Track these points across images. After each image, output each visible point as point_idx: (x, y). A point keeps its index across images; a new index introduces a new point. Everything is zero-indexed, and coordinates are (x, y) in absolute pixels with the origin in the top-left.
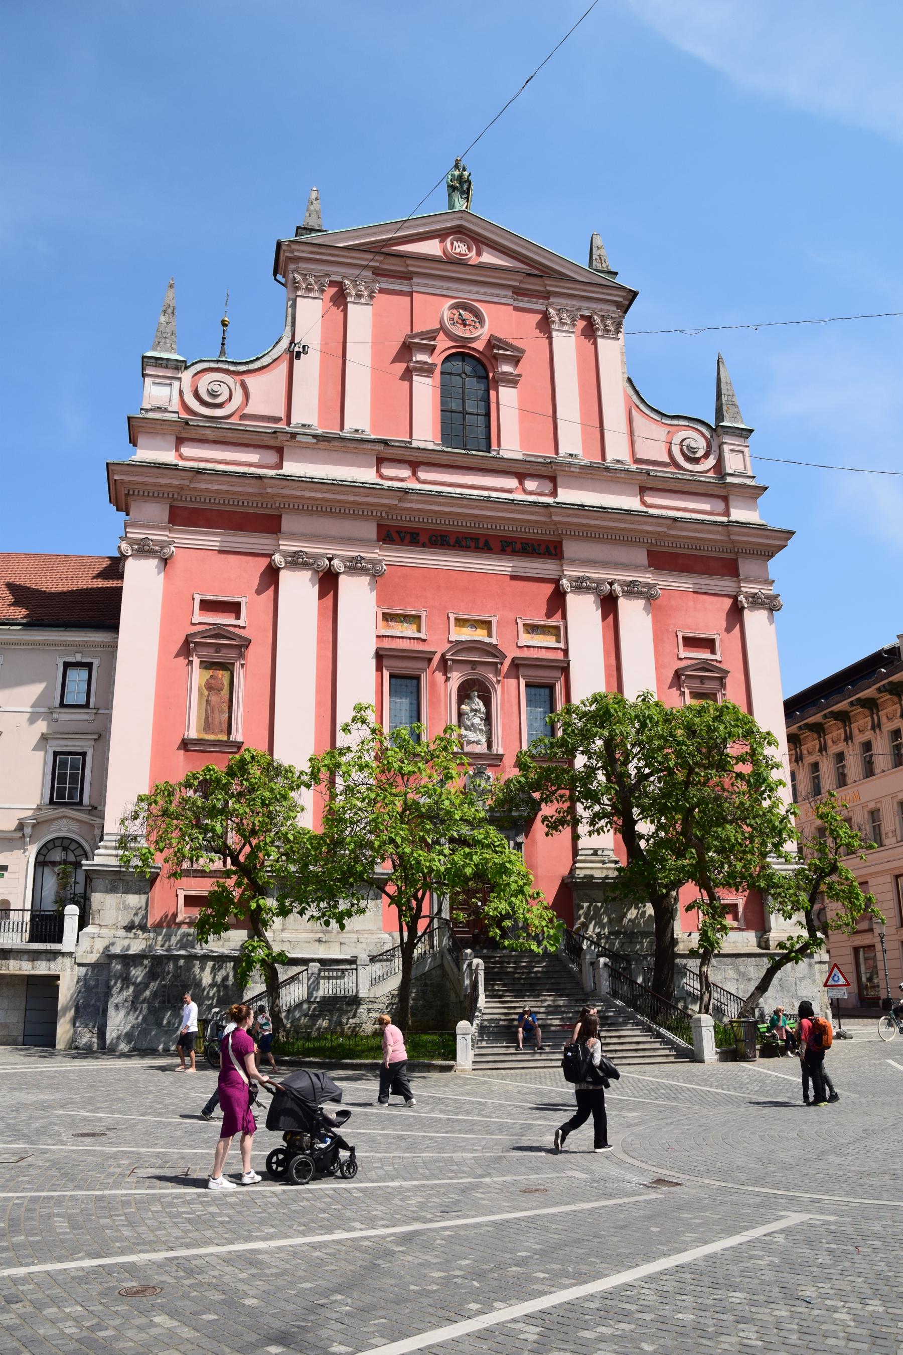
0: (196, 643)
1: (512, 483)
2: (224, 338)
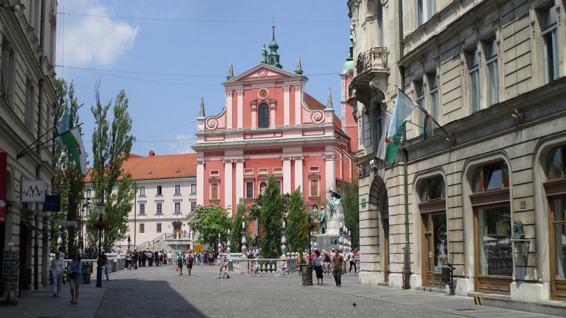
0: (210, 181)
1: (273, 135)
2: (274, 33)
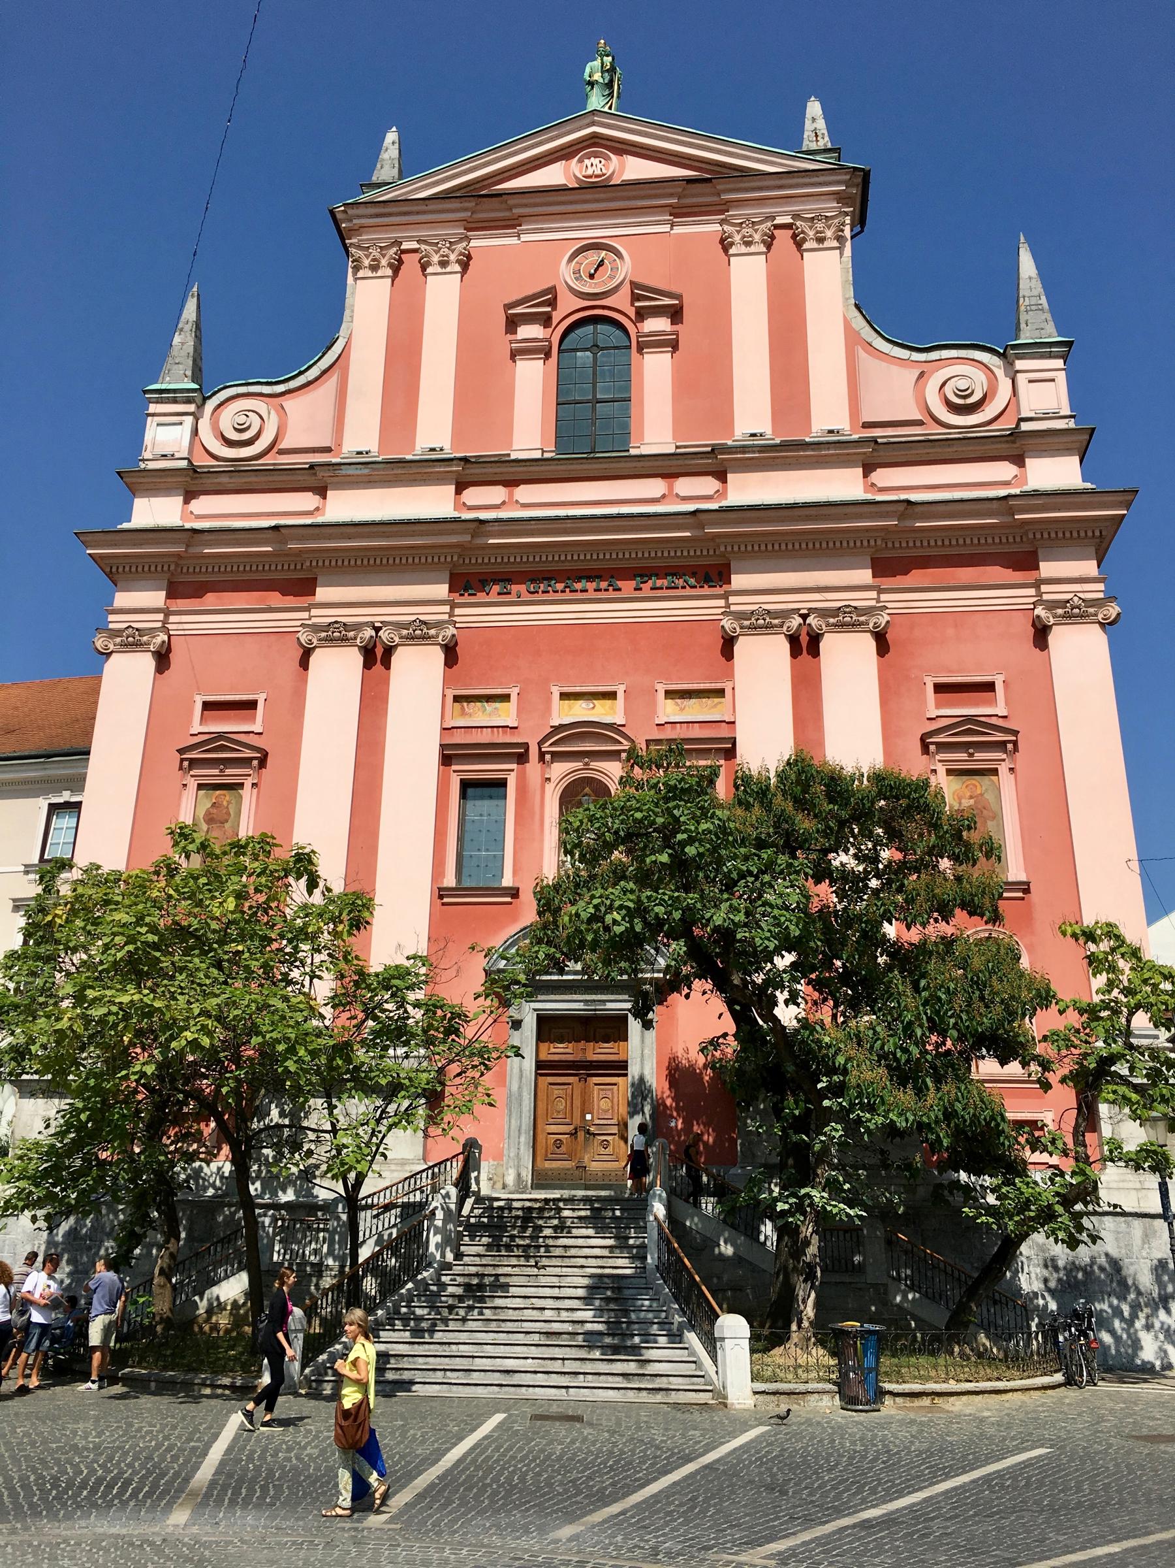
0: (192, 761)
1: (654, 487)
